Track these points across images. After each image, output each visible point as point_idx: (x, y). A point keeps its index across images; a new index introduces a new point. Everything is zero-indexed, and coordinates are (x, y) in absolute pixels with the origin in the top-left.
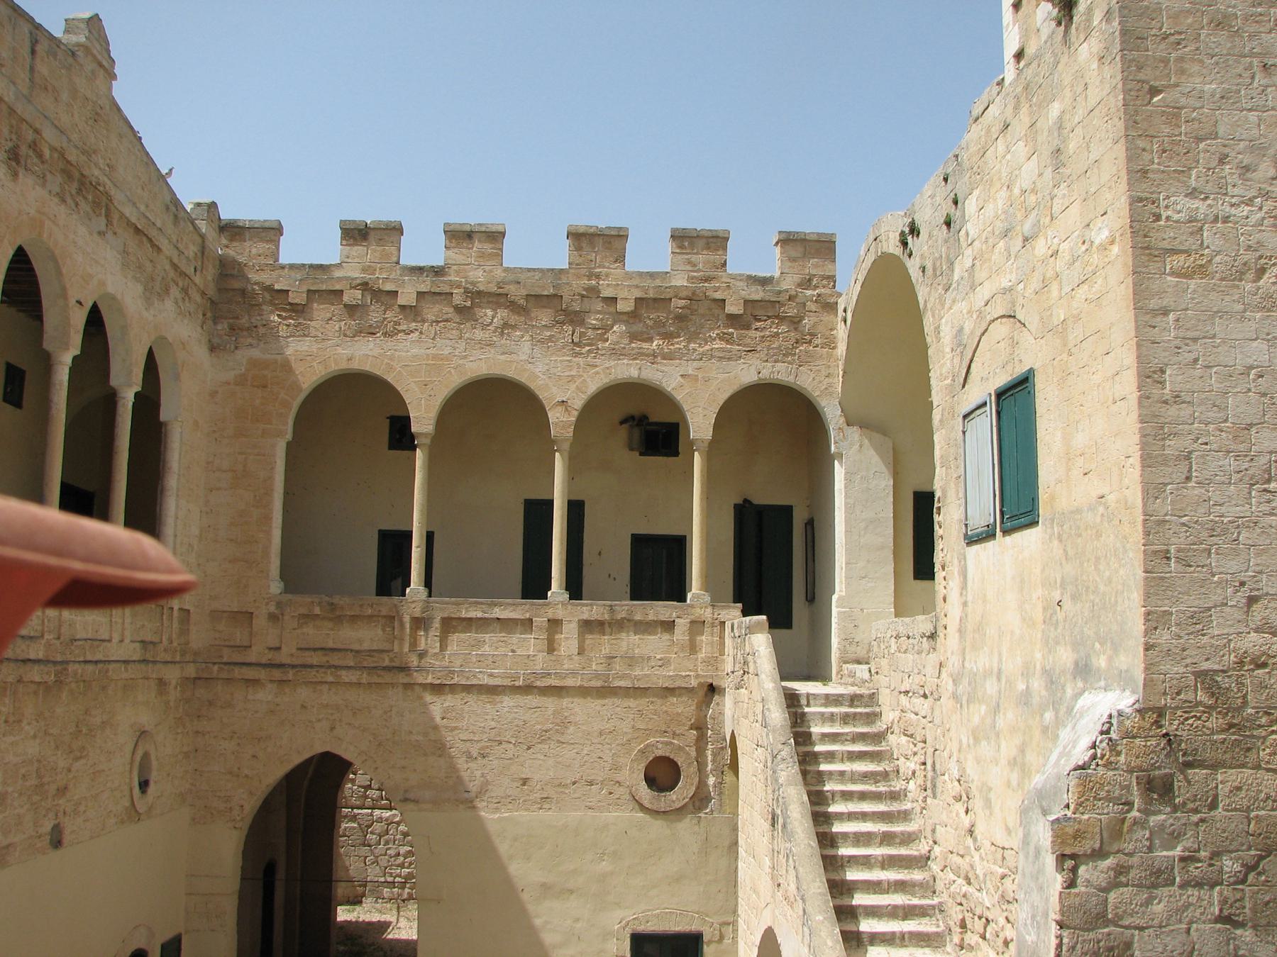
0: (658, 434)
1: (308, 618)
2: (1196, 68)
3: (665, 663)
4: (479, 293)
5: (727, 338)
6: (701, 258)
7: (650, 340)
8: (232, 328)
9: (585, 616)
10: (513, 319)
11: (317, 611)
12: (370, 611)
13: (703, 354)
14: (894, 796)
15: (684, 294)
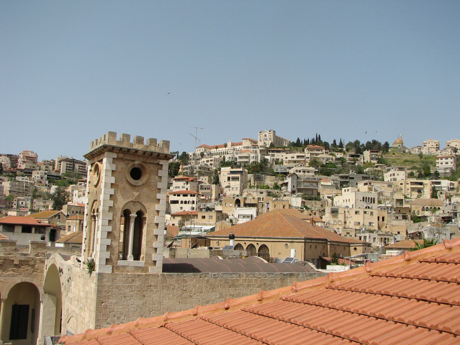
2: (111, 297)
6: (8, 248)
13: (7, 275)
15: (2, 259)
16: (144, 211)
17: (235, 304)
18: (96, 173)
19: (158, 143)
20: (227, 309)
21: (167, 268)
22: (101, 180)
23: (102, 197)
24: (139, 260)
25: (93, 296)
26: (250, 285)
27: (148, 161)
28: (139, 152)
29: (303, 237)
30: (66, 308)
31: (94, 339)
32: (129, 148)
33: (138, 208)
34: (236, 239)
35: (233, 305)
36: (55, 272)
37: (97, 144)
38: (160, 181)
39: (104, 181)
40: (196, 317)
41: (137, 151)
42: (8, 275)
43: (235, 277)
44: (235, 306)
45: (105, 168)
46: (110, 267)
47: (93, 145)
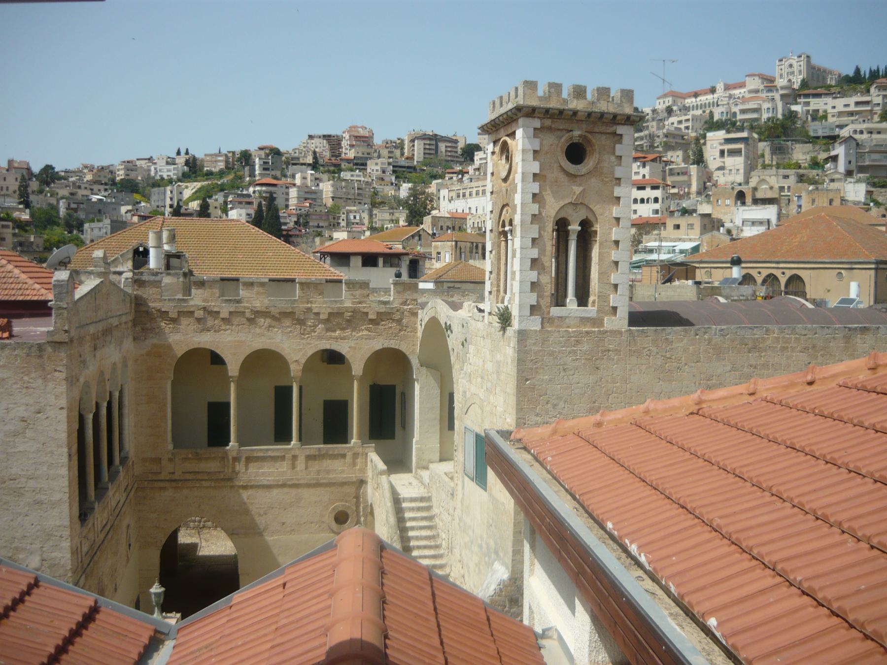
0: (333, 358)
1: (185, 459)
2: (541, 371)
3: (342, 472)
4: (258, 312)
5: (369, 330)
6: (358, 293)
7: (335, 331)
8: (143, 329)
9: (308, 453)
10: (274, 323)
11: (190, 456)
12: (213, 455)
14: (437, 547)
16: (591, 218)
17: (826, 375)
18: (504, 157)
19: (612, 95)
20: (811, 383)
21: (638, 319)
22: (513, 169)
23: (518, 199)
24: (586, 305)
25: (510, 369)
26: (787, 348)
27: (596, 130)
28: (579, 113)
29: (873, 259)
30: (461, 389)
31: (572, 435)
32: (562, 107)
33: (582, 214)
34: (743, 265)
35: (821, 376)
36: (437, 332)
37: (501, 105)
38: (620, 165)
39: (520, 170)
40: (752, 398)
41: (575, 113)
42: (361, 338)
43: (758, 334)
44: (824, 378)
45: (520, 147)
46: (537, 319)
47: (494, 107)
